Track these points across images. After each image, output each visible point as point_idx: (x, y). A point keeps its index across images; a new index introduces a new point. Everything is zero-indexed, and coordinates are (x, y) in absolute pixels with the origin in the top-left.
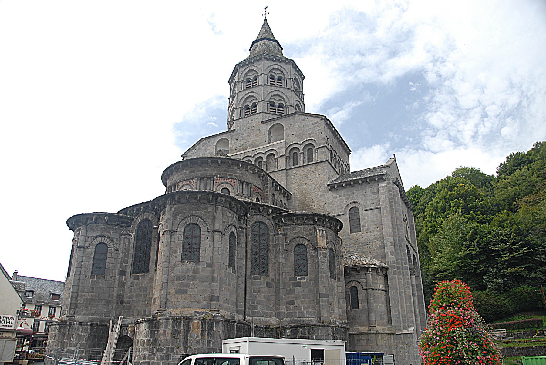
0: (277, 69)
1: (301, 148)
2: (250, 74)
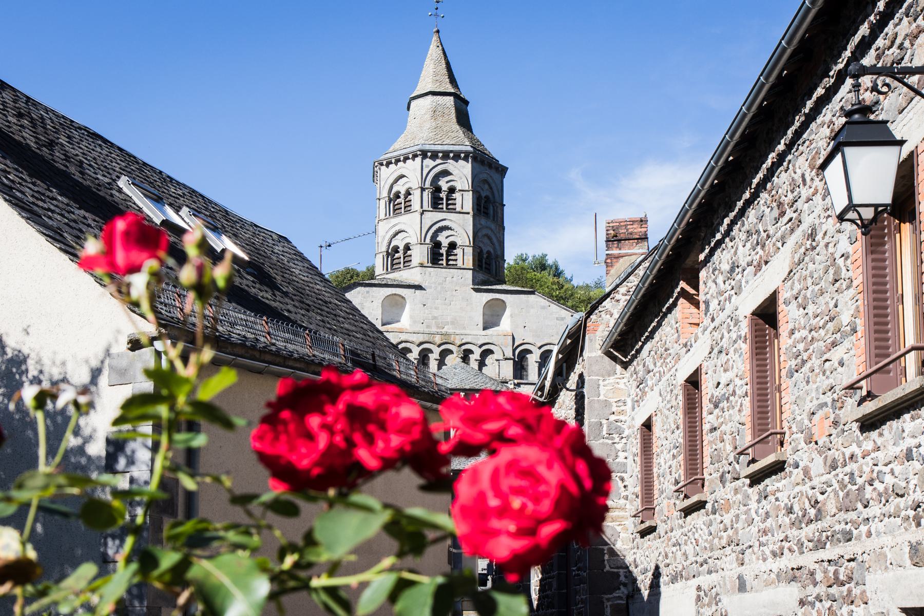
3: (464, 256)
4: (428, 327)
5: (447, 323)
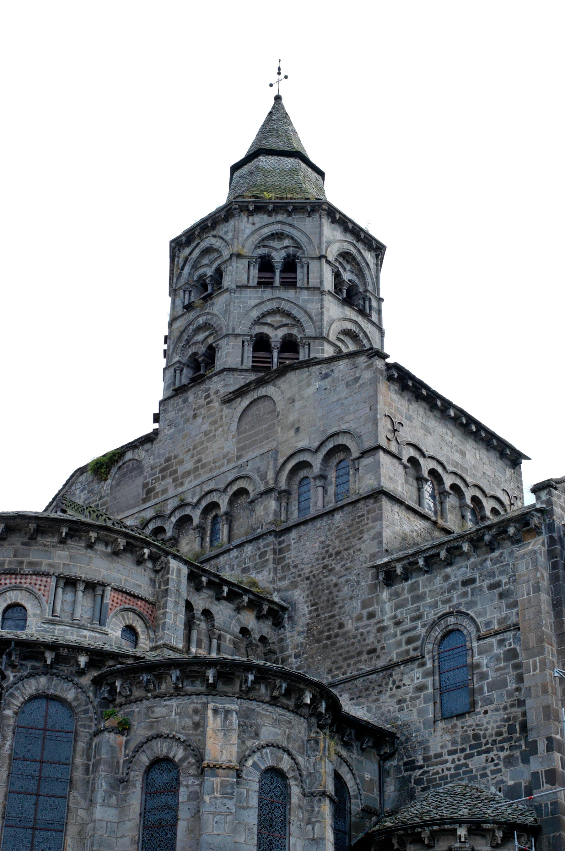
1: (317, 461)
2: (205, 261)
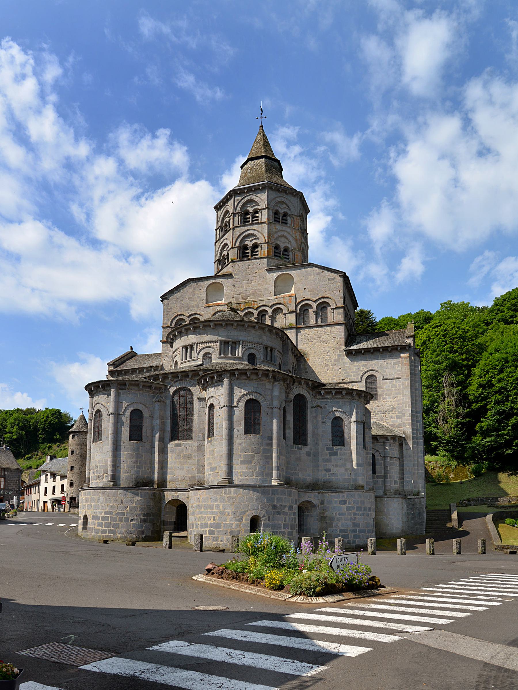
0: (282, 203)
1: (314, 305)
3: (263, 250)
4: (236, 299)
5: (249, 295)
